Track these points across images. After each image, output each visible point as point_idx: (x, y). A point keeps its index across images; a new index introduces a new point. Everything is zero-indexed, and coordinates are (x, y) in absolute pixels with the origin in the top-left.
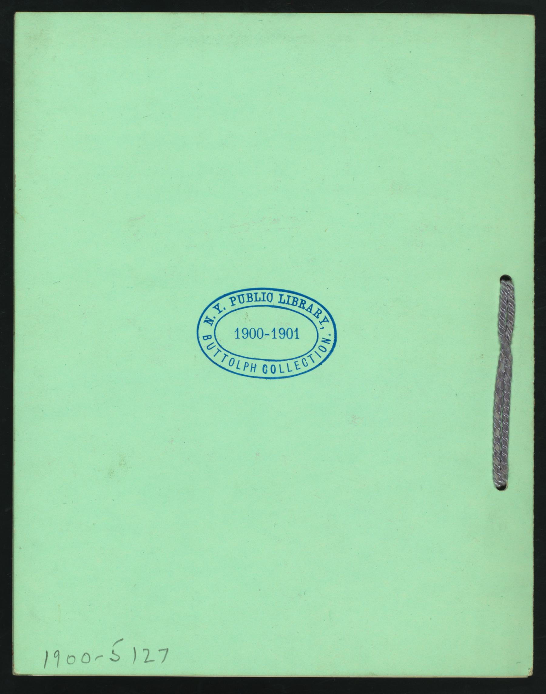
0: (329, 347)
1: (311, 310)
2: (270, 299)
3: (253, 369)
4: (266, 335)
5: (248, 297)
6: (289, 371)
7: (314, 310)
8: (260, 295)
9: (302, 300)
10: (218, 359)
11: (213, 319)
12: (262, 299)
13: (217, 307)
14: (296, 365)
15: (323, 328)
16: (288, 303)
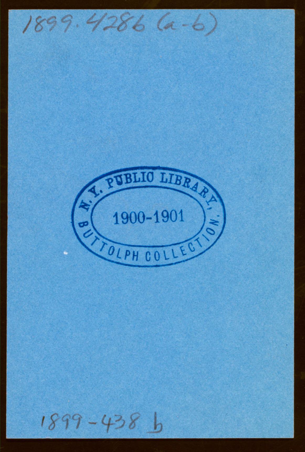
0: (218, 229)
1: (196, 188)
2: (150, 178)
3: (135, 257)
4: (148, 218)
5: (127, 178)
6: (175, 257)
7: (200, 189)
8: (139, 176)
9: (187, 179)
10: (96, 247)
11: (89, 203)
12: (141, 180)
13: (93, 191)
14: (182, 251)
15: (210, 208)
16: (170, 183)
